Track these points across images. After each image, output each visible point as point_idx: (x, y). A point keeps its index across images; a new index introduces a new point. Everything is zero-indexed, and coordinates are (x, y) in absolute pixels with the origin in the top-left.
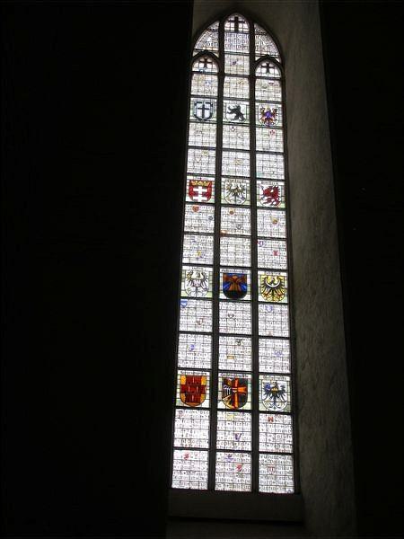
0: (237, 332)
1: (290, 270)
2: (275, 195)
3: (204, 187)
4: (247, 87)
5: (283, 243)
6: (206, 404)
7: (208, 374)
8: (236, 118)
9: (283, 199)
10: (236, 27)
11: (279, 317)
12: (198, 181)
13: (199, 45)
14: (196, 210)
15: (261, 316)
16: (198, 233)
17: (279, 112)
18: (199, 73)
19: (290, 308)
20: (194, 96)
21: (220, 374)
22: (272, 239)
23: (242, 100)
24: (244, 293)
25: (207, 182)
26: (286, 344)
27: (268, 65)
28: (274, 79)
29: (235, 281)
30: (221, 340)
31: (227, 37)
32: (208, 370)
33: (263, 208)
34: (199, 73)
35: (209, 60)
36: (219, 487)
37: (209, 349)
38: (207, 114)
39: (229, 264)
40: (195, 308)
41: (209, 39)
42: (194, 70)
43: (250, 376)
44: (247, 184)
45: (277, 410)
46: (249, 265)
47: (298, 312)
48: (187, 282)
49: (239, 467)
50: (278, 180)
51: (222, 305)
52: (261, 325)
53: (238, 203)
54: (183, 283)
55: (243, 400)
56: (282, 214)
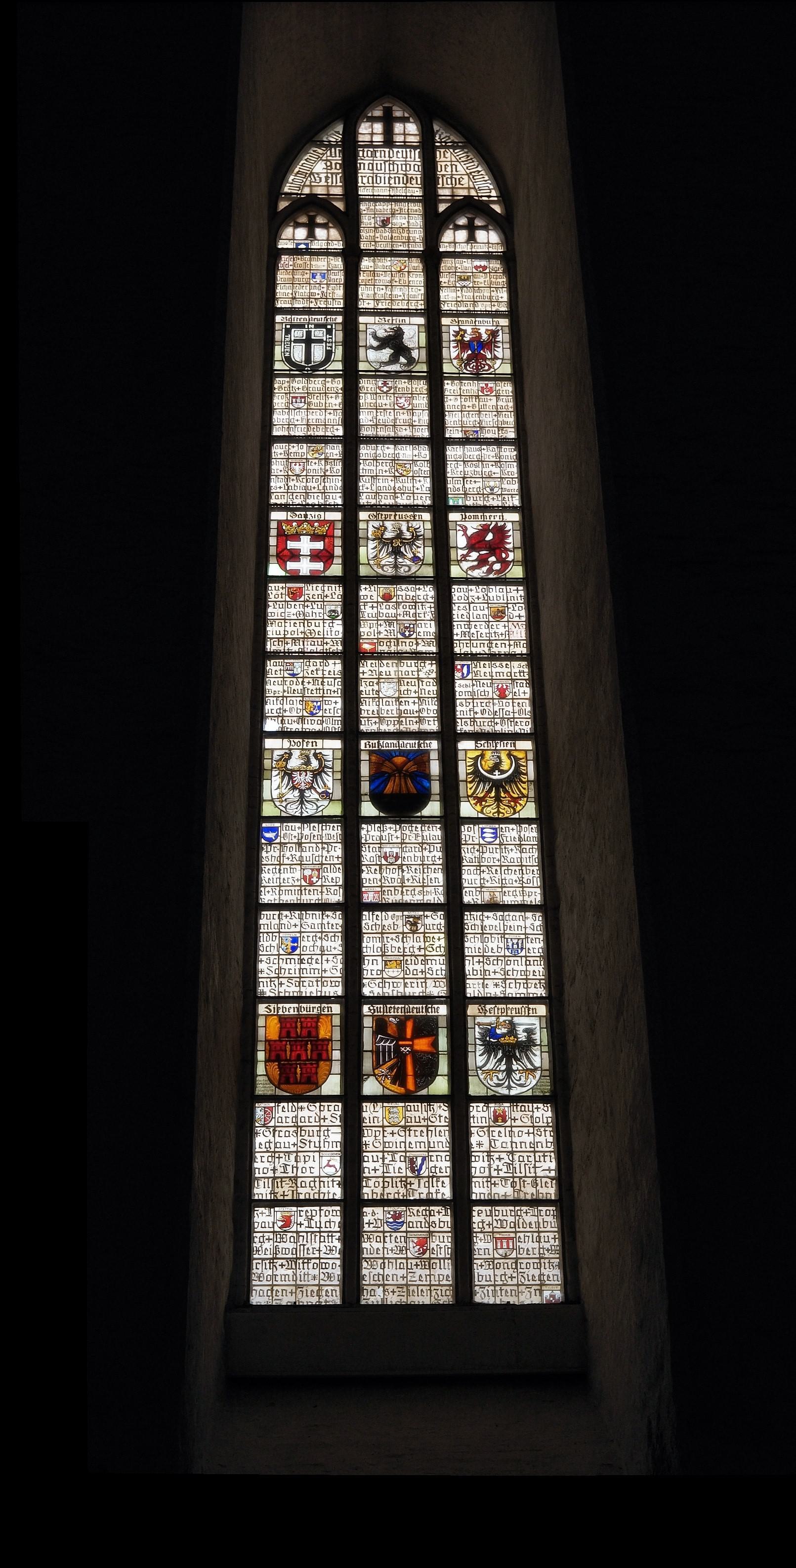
0: (408, 898)
1: (539, 735)
2: (497, 547)
3: (315, 537)
4: (419, 279)
5: (520, 669)
6: (332, 1085)
7: (336, 1008)
8: (394, 359)
9: (519, 555)
10: (388, 133)
11: (514, 855)
12: (300, 523)
13: (292, 184)
14: (295, 595)
15: (467, 854)
16: (303, 655)
17: (503, 337)
18: (295, 252)
19: (541, 831)
20: (283, 311)
21: (366, 1009)
22: (493, 657)
23: (408, 313)
24: (424, 798)
25: (322, 522)
26: (534, 922)
27: (471, 222)
28: (488, 256)
29: (399, 769)
30: (368, 920)
31: (365, 159)
32: (336, 999)
33: (467, 581)
34: (295, 252)
35: (320, 220)
36: (373, 1296)
37: (336, 945)
38: (318, 353)
39: (384, 728)
40: (299, 844)
41: (320, 167)
42: (282, 245)
43: (443, 1010)
44: (424, 522)
45: (513, 1092)
46: (433, 726)
47: (560, 839)
48: (276, 781)
49: (423, 1243)
50: (505, 509)
51: (369, 833)
52: (469, 877)
53: (402, 571)
54: (266, 784)
55: (427, 1072)
56: (517, 594)
